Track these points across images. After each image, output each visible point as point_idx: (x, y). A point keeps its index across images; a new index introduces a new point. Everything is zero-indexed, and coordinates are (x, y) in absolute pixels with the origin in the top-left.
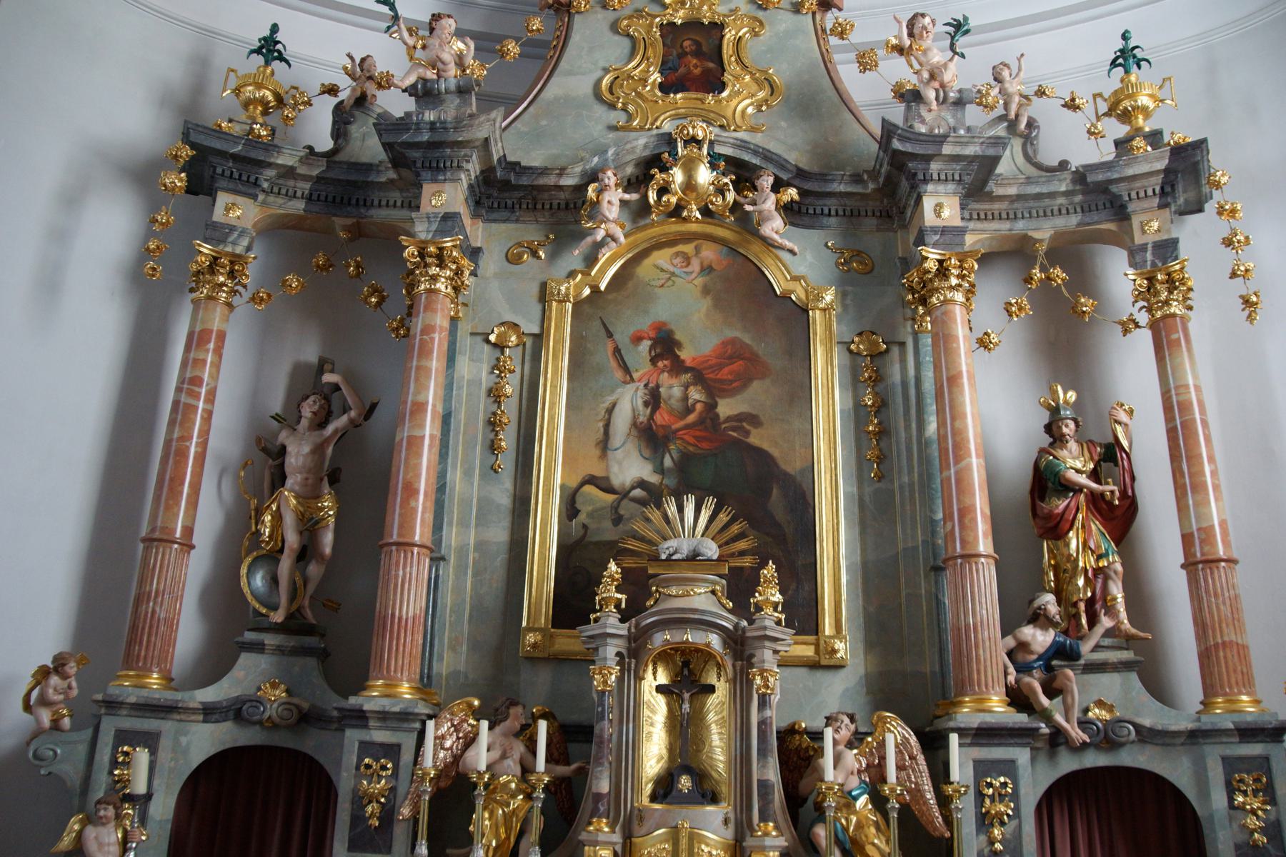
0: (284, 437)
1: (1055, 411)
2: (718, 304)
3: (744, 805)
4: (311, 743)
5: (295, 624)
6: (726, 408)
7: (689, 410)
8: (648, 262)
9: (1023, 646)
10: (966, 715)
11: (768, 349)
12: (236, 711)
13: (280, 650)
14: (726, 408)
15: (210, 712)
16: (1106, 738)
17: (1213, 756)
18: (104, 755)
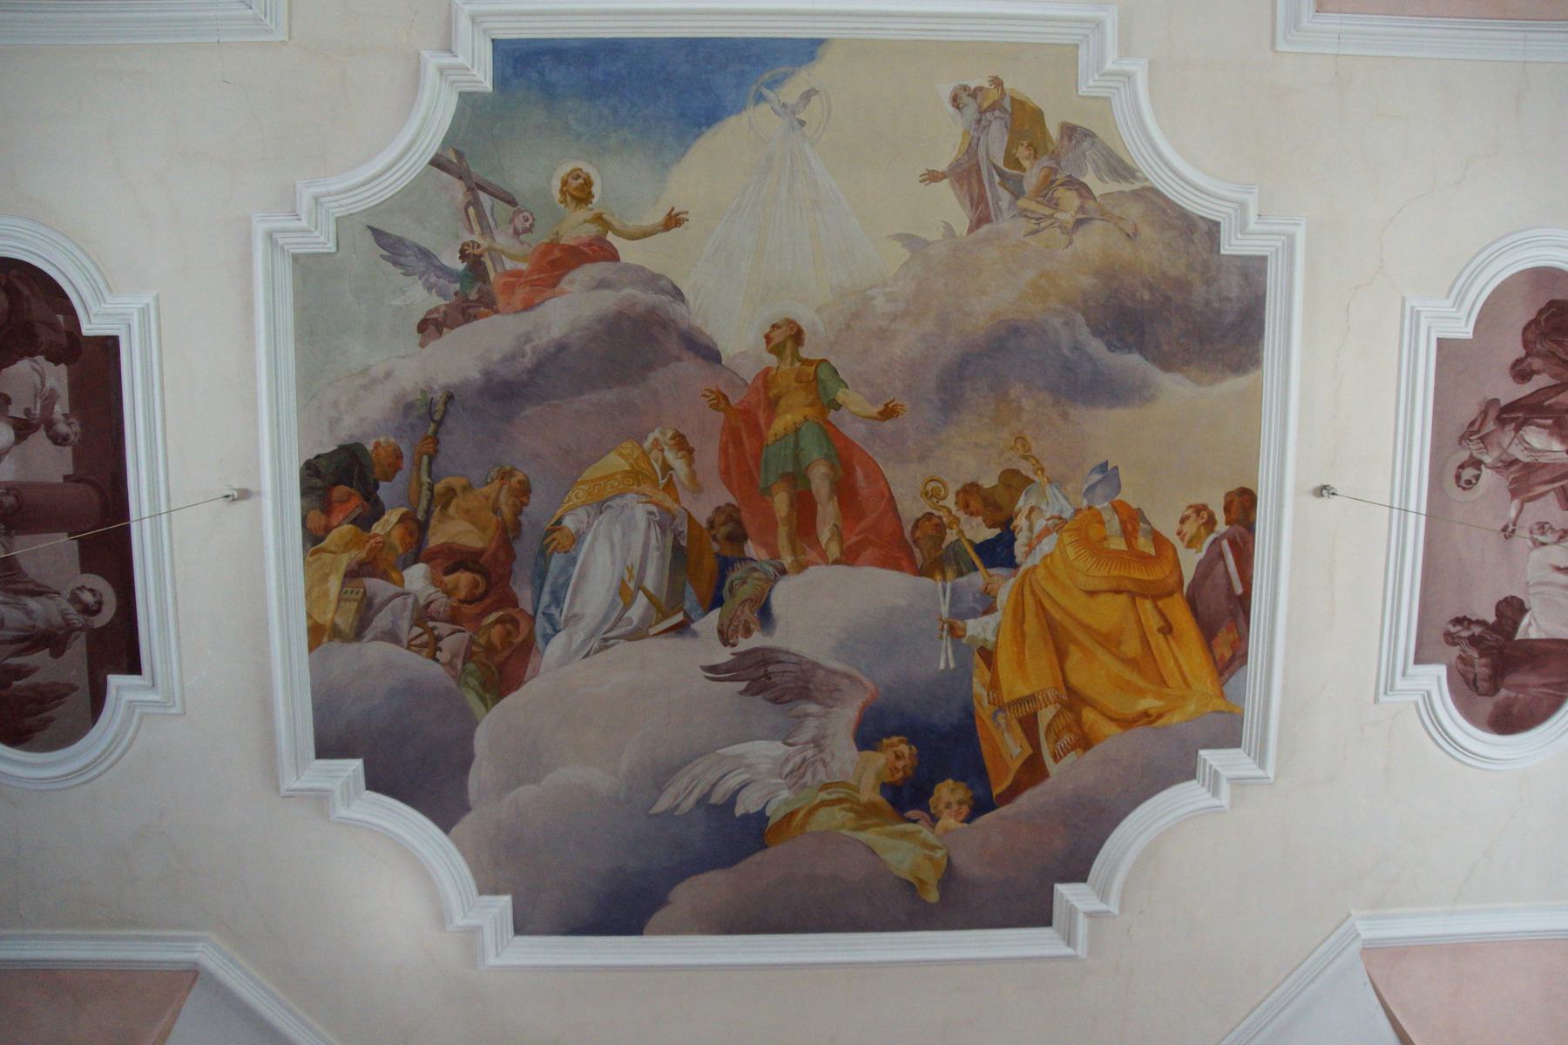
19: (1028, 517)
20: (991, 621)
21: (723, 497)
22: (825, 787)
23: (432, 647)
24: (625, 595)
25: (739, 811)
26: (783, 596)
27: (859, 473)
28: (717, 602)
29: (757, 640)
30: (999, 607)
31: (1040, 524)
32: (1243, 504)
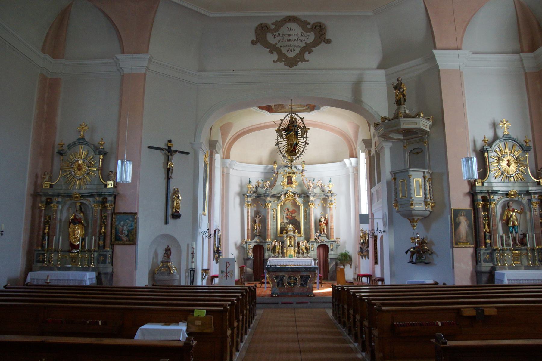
0: (255, 219)
2: (292, 206)
3: (295, 247)
4: (261, 244)
5: (259, 235)
6: (293, 215)
7: (290, 216)
8: (286, 202)
9: (317, 235)
10: (311, 240)
11: (297, 210)
12: (256, 242)
13: (259, 237)
14: (293, 215)
15: (254, 242)
16: (323, 242)
17: (330, 243)
18: (248, 246)
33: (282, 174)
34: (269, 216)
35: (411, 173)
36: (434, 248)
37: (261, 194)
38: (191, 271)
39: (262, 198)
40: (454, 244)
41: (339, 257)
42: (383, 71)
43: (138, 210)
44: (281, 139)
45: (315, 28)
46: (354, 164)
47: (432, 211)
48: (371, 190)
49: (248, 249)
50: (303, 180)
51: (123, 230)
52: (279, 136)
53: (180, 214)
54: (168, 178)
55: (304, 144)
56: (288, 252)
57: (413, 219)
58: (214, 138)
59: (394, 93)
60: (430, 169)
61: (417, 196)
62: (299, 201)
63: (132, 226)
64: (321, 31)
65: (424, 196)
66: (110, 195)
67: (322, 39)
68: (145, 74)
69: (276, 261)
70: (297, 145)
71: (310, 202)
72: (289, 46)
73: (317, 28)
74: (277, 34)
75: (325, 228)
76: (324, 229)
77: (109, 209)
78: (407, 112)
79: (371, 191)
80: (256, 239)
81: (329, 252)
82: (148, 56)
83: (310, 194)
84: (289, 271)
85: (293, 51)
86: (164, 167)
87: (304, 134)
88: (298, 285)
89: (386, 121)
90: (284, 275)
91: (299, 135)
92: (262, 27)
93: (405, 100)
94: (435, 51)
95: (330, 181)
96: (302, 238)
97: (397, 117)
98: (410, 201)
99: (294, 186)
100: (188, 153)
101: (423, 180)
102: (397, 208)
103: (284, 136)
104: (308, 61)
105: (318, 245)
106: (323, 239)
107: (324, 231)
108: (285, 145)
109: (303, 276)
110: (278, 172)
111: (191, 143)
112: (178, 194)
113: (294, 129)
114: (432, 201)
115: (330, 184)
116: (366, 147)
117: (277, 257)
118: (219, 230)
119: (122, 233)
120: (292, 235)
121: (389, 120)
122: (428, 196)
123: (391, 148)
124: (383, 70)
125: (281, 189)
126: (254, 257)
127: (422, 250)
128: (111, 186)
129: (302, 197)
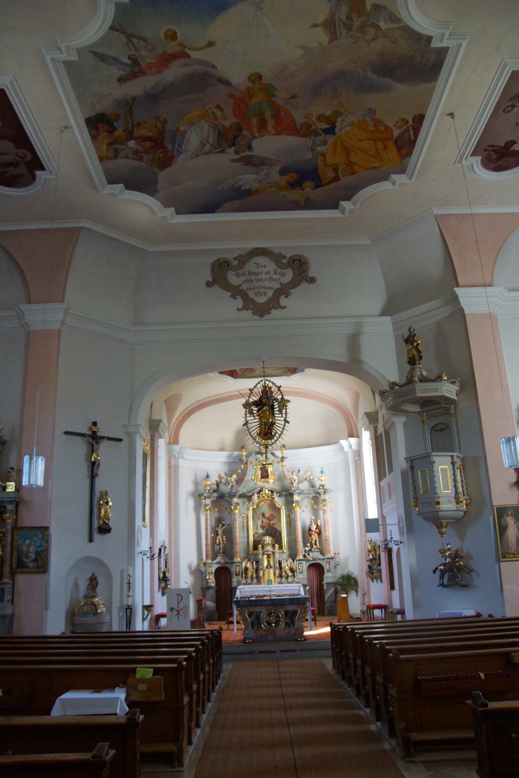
0: (217, 529)
1: (311, 520)
3: (275, 568)
4: (227, 566)
5: (224, 553)
6: (271, 523)
10: (298, 558)
12: (219, 563)
14: (271, 523)
15: (216, 563)
16: (314, 560)
17: (325, 561)
19: (341, 122)
20: (325, 147)
21: (234, 120)
22: (270, 183)
23: (141, 159)
24: (203, 145)
25: (242, 189)
26: (255, 144)
27: (282, 113)
28: (233, 145)
29: (247, 153)
30: (328, 143)
31: (345, 124)
32: (419, 119)
33: (254, 463)
34: (236, 525)
35: (435, 459)
36: (473, 564)
37: (224, 494)
38: (126, 609)
39: (226, 498)
40: (501, 557)
41: (340, 580)
42: (388, 319)
43: (50, 523)
44: (250, 416)
45: (293, 263)
46: (354, 447)
47: (466, 511)
48: (380, 483)
49: (207, 573)
50: (283, 472)
51: (28, 551)
52: (247, 413)
53: (111, 527)
54: (93, 477)
55: (283, 423)
56: (266, 576)
57: (441, 523)
58: (156, 417)
59: (405, 348)
60: (460, 452)
61: (444, 490)
62: (279, 502)
63: (41, 546)
64: (301, 266)
65: (454, 490)
66: (11, 502)
67: (303, 278)
68: (60, 331)
69: (249, 589)
70: (273, 424)
71: (295, 502)
72: (258, 288)
73: (296, 262)
74: (241, 272)
75: (318, 539)
76: (316, 541)
77: (9, 523)
78: (424, 373)
79: (380, 485)
80: (219, 559)
81: (323, 574)
82: (65, 306)
83: (295, 491)
84: (268, 605)
85: (263, 295)
86: (86, 461)
87: (283, 409)
88: (282, 625)
89: (396, 387)
90: (260, 611)
91: (275, 410)
92: (221, 264)
93: (421, 357)
94: (457, 290)
95: (322, 472)
96: (285, 556)
97: (410, 381)
98: (435, 499)
99: (271, 481)
100: (120, 440)
101: (452, 468)
102: (417, 509)
103: (255, 412)
104: (285, 307)
105: (308, 564)
106: (316, 555)
107: (316, 544)
108: (256, 425)
109: (288, 611)
110: (247, 461)
111: (125, 426)
112: (106, 499)
113: (269, 402)
114: (466, 497)
115: (322, 476)
116: (370, 423)
117: (250, 584)
118: (166, 548)
119: (27, 557)
120: (269, 551)
121: (400, 386)
122: (460, 490)
123: (405, 424)
124: (389, 317)
125: (252, 485)
126: (216, 585)
127: (457, 567)
128: (12, 489)
129: (284, 496)
